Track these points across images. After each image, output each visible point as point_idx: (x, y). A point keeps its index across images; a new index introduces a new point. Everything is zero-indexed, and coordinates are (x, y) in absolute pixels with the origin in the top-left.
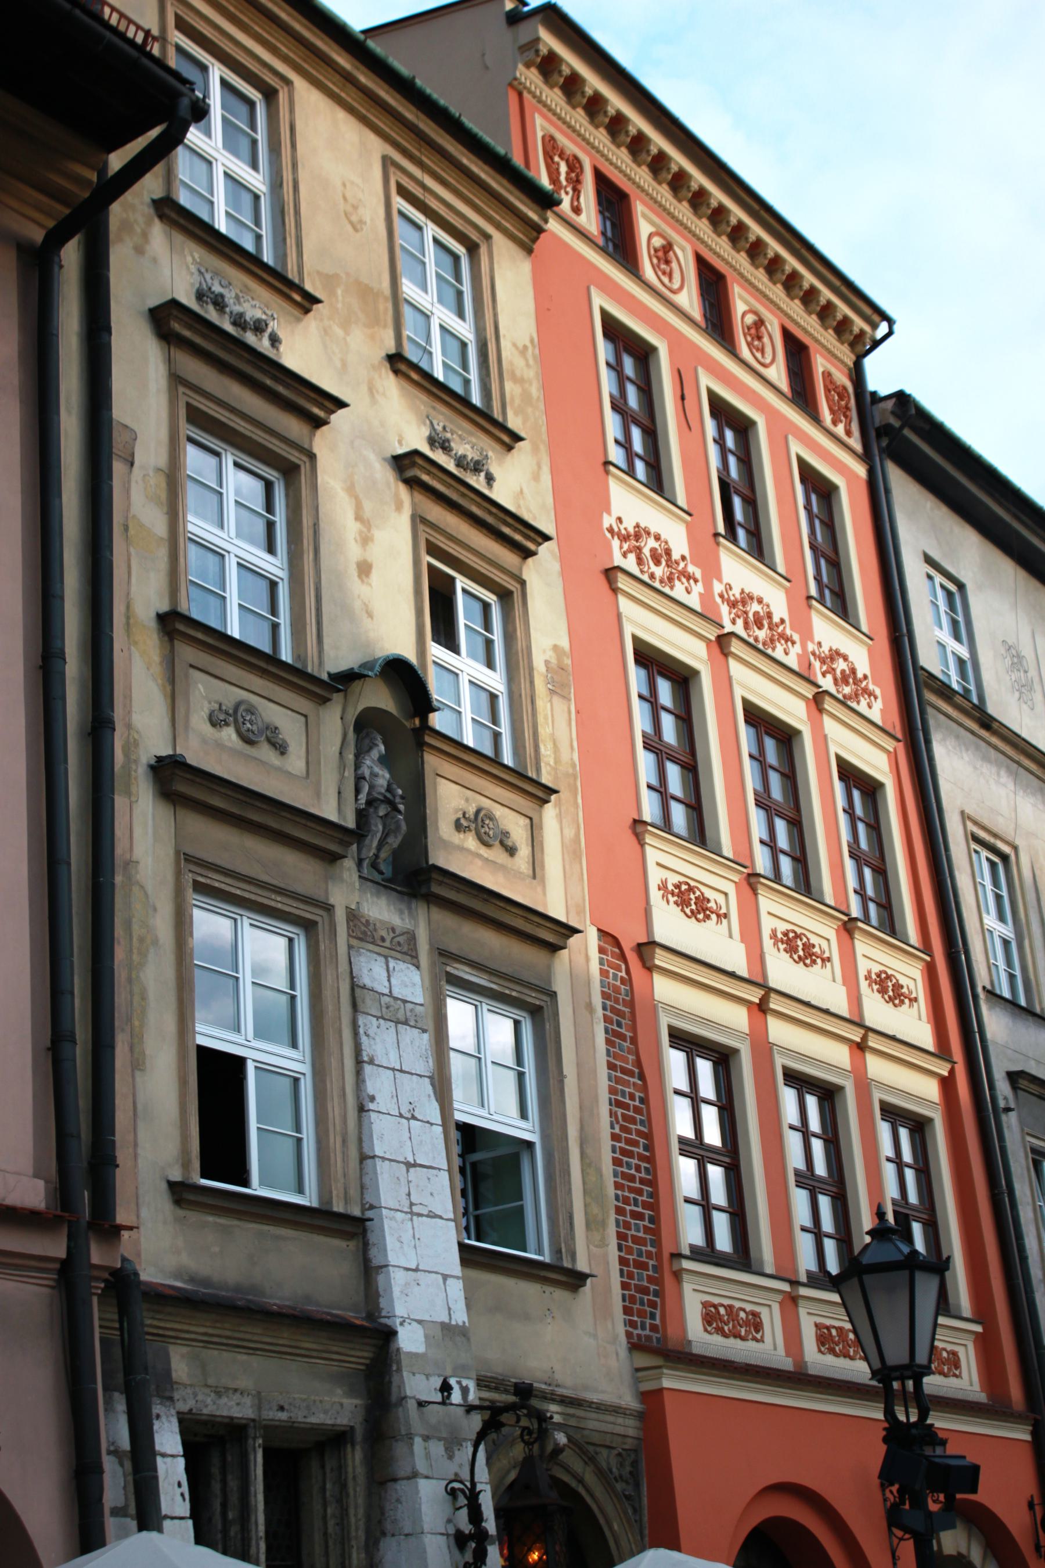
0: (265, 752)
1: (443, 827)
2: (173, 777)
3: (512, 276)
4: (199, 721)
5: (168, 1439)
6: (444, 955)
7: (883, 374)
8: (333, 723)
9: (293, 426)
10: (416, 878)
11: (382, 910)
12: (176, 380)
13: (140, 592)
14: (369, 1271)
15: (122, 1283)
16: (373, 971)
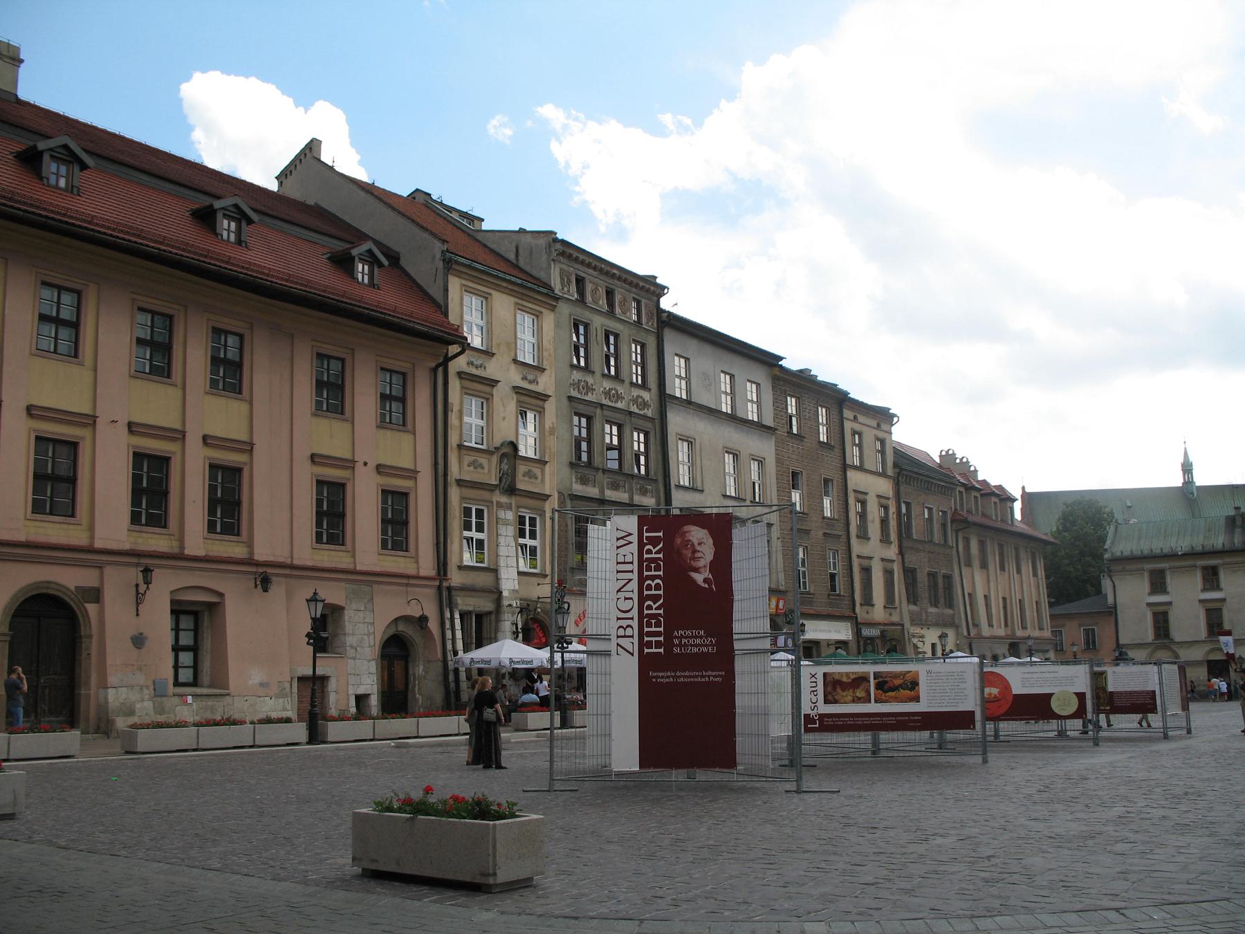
0: (479, 470)
1: (519, 476)
2: (460, 483)
3: (549, 319)
4: (466, 468)
5: (457, 616)
6: (518, 507)
7: (666, 303)
8: (495, 459)
9: (487, 389)
10: (511, 490)
11: (504, 499)
12: (463, 387)
13: (453, 440)
14: (497, 579)
15: (449, 589)
16: (502, 514)
